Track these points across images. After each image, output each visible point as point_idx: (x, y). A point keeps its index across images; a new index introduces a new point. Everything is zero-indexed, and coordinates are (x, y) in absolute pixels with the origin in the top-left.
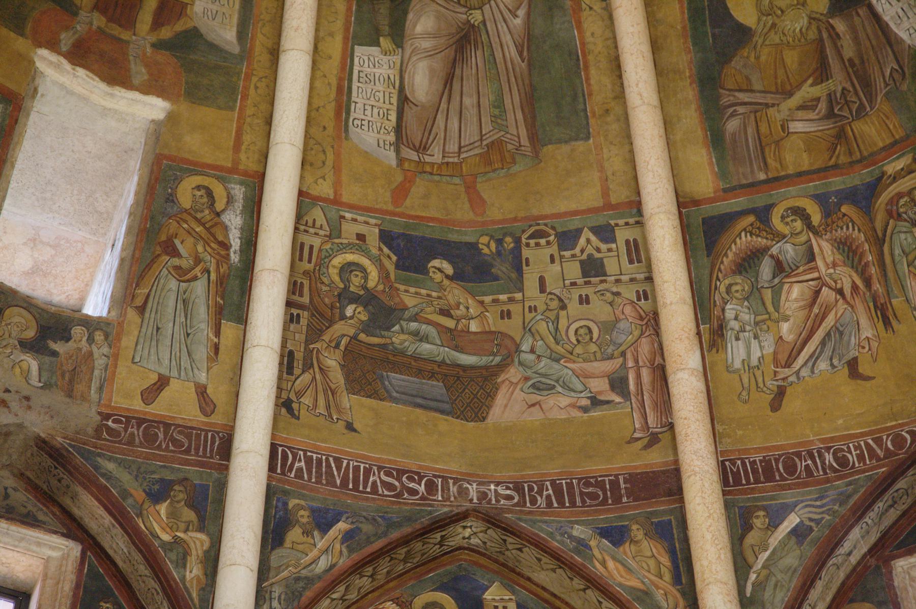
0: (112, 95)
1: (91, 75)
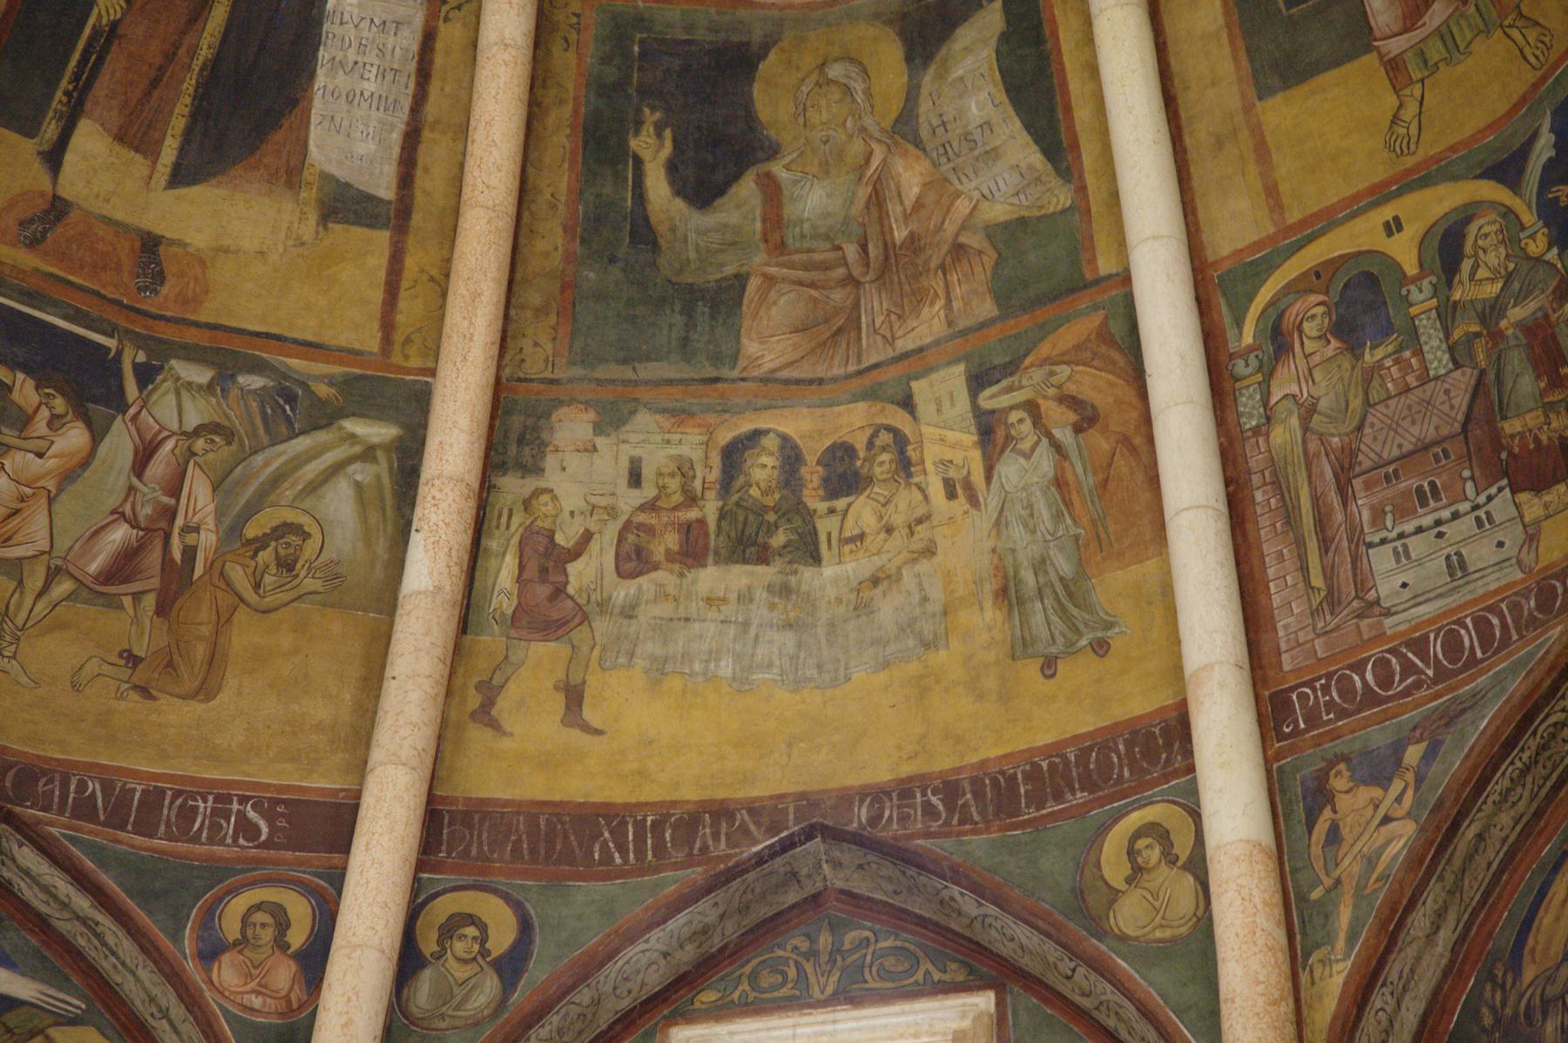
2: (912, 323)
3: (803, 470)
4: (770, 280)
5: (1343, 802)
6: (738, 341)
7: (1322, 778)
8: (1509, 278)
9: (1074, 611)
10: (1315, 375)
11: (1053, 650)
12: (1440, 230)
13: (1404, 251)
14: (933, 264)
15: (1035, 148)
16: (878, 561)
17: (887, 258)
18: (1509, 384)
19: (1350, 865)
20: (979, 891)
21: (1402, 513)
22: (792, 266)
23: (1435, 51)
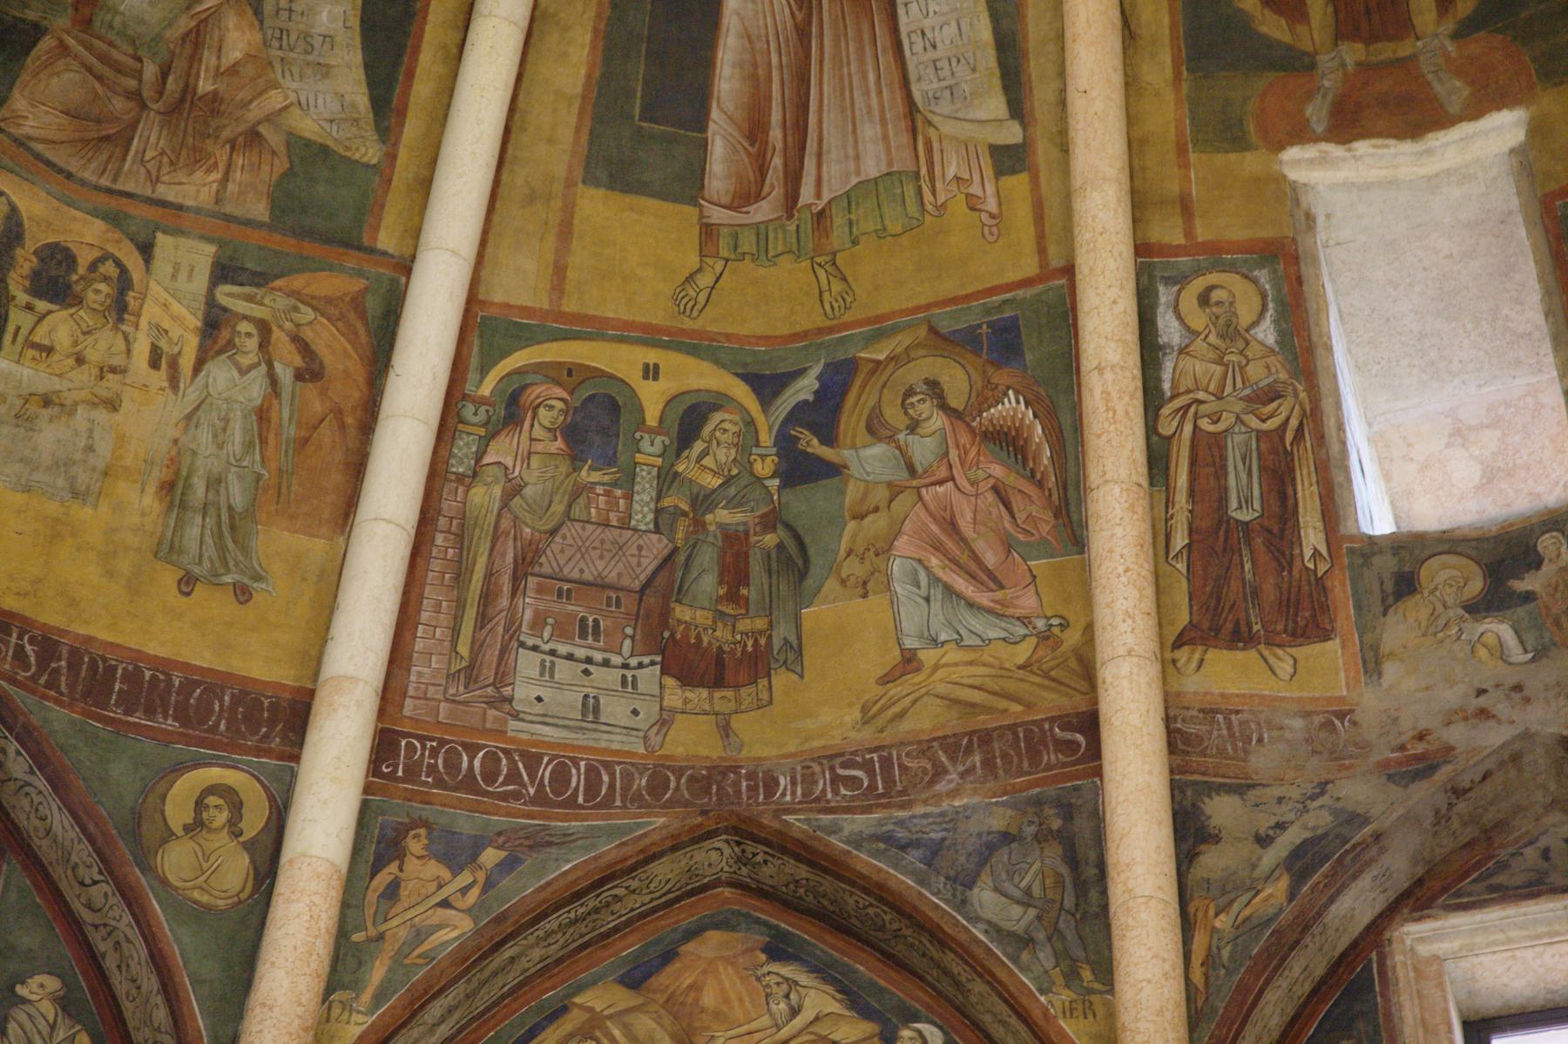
0: (1428, 152)
1: (1379, 142)
2: (181, 176)
3: (19, 251)
4: (63, 48)
5: (412, 865)
6: (10, 89)
7: (402, 832)
8: (729, 481)
9: (231, 545)
10: (529, 457)
11: (196, 570)
12: (689, 401)
13: (652, 398)
14: (226, 134)
15: (364, 89)
16: (57, 384)
17: (182, 100)
18: (694, 574)
19: (397, 928)
20: (41, 759)
21: (561, 632)
22: (89, 48)
23: (748, 243)
